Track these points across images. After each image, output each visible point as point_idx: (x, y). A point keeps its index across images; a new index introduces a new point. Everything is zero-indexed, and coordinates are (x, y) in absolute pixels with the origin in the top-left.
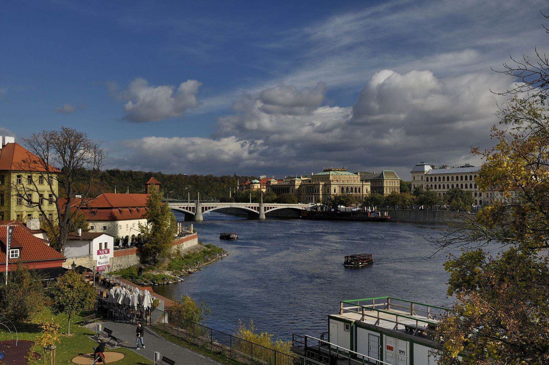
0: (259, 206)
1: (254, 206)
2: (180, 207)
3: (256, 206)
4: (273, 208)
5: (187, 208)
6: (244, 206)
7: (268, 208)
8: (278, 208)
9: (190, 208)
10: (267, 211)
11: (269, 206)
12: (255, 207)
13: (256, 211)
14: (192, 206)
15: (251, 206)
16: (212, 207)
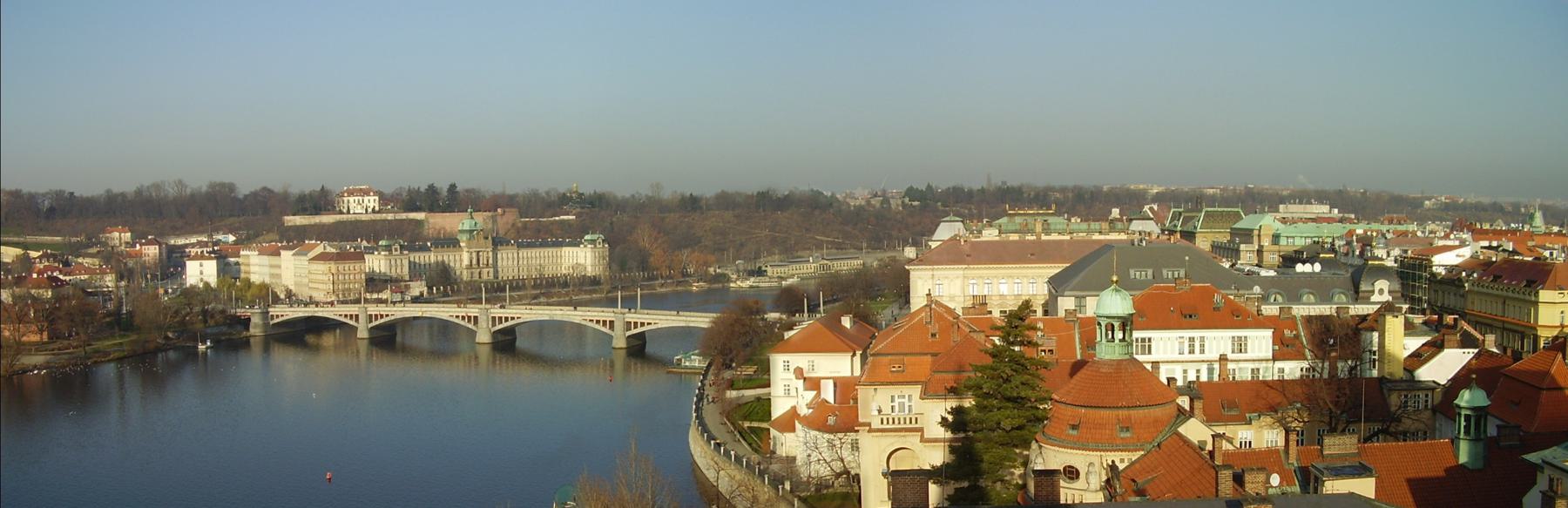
0: (613, 319)
1: (601, 319)
3: (608, 319)
4: (649, 324)
5: (463, 318)
6: (579, 318)
7: (636, 323)
8: (660, 326)
9: (469, 317)
10: (634, 331)
11: (639, 321)
12: (605, 322)
13: (606, 330)
14: (472, 315)
15: (595, 319)
16: (513, 318)
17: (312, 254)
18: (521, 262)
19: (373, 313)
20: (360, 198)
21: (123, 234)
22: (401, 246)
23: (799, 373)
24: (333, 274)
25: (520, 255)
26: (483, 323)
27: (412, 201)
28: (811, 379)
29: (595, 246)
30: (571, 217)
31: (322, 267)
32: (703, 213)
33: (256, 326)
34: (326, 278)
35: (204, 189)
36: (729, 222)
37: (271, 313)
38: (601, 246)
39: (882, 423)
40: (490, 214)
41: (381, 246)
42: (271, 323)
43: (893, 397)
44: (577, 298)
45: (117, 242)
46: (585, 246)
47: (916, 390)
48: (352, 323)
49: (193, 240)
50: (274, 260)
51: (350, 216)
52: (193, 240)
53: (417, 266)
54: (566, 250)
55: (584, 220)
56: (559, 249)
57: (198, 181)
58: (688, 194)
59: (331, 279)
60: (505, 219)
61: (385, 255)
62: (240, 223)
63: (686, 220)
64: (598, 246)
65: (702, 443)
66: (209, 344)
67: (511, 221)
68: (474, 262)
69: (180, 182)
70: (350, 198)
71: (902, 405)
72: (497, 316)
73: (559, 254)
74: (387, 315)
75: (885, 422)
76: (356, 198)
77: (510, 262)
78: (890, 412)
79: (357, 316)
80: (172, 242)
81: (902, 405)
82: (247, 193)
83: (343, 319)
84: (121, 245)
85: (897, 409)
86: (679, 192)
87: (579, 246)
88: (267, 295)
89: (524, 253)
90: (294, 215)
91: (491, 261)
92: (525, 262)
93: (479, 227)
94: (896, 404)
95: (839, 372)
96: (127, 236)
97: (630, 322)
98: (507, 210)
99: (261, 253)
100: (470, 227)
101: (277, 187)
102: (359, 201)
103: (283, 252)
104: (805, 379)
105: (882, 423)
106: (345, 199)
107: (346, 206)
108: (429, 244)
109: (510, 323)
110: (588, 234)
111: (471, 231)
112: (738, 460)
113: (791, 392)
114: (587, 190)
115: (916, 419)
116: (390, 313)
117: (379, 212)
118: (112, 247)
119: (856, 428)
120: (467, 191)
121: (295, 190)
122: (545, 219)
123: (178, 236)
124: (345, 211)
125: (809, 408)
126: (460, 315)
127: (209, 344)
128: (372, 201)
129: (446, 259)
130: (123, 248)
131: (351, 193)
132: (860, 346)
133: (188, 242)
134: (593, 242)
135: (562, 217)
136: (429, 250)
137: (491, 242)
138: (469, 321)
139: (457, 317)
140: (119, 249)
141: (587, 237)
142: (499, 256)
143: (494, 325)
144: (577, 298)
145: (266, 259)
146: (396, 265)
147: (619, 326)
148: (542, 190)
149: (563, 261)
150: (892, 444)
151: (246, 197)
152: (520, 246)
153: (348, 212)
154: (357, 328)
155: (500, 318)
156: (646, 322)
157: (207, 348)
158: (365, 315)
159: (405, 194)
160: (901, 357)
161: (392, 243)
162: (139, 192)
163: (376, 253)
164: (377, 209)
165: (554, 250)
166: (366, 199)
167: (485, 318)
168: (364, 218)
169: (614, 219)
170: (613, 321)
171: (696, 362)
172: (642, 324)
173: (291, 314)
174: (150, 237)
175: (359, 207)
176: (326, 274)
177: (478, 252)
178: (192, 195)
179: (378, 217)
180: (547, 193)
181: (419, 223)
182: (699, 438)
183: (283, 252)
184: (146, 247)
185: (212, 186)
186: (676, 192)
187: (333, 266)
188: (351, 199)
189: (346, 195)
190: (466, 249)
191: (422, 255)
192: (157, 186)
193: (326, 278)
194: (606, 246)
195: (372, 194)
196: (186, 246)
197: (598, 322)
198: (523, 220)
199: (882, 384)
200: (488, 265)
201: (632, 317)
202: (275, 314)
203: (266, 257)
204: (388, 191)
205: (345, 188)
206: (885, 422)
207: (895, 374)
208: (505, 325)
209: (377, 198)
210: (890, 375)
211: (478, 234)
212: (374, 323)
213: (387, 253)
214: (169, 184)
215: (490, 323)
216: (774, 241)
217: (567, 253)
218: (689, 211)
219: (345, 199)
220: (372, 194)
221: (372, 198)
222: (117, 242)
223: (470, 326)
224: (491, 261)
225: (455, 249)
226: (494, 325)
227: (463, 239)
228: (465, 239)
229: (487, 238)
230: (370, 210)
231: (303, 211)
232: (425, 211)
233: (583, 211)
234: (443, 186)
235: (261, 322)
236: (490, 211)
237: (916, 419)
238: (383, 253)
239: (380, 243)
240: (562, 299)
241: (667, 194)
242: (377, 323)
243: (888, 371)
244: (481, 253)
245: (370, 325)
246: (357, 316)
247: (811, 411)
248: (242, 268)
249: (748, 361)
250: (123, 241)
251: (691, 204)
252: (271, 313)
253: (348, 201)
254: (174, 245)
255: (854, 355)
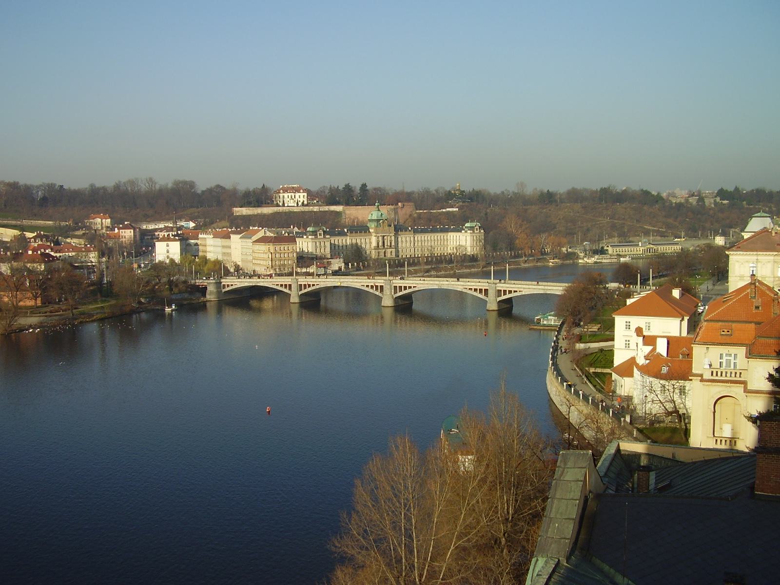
1: (478, 288)
2: (362, 285)
4: (515, 291)
5: (372, 287)
7: (505, 291)
8: (523, 293)
9: (377, 287)
10: (503, 297)
11: (507, 289)
12: (481, 290)
13: (482, 296)
14: (379, 285)
16: (410, 287)
17: (255, 238)
18: (416, 244)
19: (303, 283)
20: (293, 194)
21: (104, 220)
22: (324, 231)
23: (639, 331)
24: (271, 253)
25: (416, 239)
26: (387, 291)
27: (333, 197)
28: (649, 337)
29: (474, 232)
30: (455, 209)
31: (263, 247)
32: (557, 206)
33: (211, 293)
34: (266, 256)
35: (170, 185)
36: (578, 212)
37: (223, 283)
38: (478, 231)
39: (712, 375)
40: (392, 207)
41: (309, 231)
42: (223, 291)
43: (721, 355)
44: (459, 271)
45: (99, 227)
46: (466, 232)
47: (741, 351)
48: (286, 291)
49: (162, 226)
50: (225, 242)
51: (285, 208)
52: (162, 226)
53: (337, 248)
54: (452, 235)
55: (465, 211)
56: (445, 234)
57: (165, 179)
58: (546, 191)
59: (270, 257)
60: (404, 211)
61: (312, 239)
62: (199, 213)
63: (544, 210)
64: (476, 232)
65: (556, 384)
66: (174, 307)
67: (408, 213)
68: (381, 244)
69: (151, 179)
70: (284, 194)
71: (728, 363)
72: (398, 285)
73: (445, 238)
74: (313, 285)
75: (714, 374)
76: (290, 194)
77: (408, 244)
78: (719, 367)
79: (290, 286)
80: (144, 227)
81: (728, 363)
82: (204, 189)
83: (279, 288)
84: (102, 228)
85: (724, 364)
86: (538, 189)
87: (461, 232)
88: (220, 269)
89: (419, 237)
90: (241, 207)
91: (393, 244)
92: (420, 244)
93: (384, 217)
94: (724, 361)
95: (670, 332)
96: (108, 222)
97: (501, 290)
98: (406, 204)
99: (216, 236)
100: (377, 217)
101: (228, 185)
102: (291, 197)
103: (232, 236)
104: (644, 337)
105: (712, 375)
106: (281, 195)
107: (281, 200)
108: (346, 230)
109: (408, 291)
110: (468, 222)
111: (378, 221)
112: (586, 398)
113: (630, 345)
114: (468, 188)
115: (741, 373)
116: (316, 284)
117: (307, 205)
118: (95, 230)
119: (690, 378)
120: (375, 189)
121: (242, 187)
122: (435, 211)
123: (149, 222)
124: (281, 204)
125: (646, 359)
126: (370, 285)
127: (174, 307)
128: (302, 197)
129: (358, 241)
130: (104, 231)
131: (285, 190)
132: (688, 313)
133: (157, 227)
134: (472, 228)
135: (447, 209)
136: (345, 234)
137: (393, 229)
138: (377, 289)
139: (367, 286)
140: (101, 232)
141: (467, 225)
142: (400, 239)
143: (395, 292)
144: (459, 271)
145: (219, 242)
146: (320, 246)
147: (491, 293)
148: (432, 189)
149: (449, 243)
150: (719, 392)
151: (203, 192)
152: (416, 232)
153: (284, 205)
154: (290, 295)
155: (400, 287)
156: (513, 290)
157: (172, 311)
158: (296, 285)
159: (327, 191)
160: (730, 324)
161: (317, 229)
162: (117, 187)
163: (305, 237)
164: (306, 202)
165: (442, 235)
166: (297, 195)
167: (389, 287)
168: (296, 210)
169: (488, 211)
170: (487, 290)
171: (552, 320)
172: (510, 292)
173: (238, 284)
174: (126, 223)
175: (292, 201)
176: (266, 253)
177: (384, 236)
178: (161, 190)
179: (306, 209)
180: (437, 191)
181: (338, 214)
182: (554, 380)
183: (232, 236)
184: (123, 230)
185: (177, 183)
186: (536, 189)
187: (272, 247)
188: (286, 195)
189: (281, 191)
190: (374, 234)
191: (340, 238)
192: (132, 183)
193: (266, 256)
194: (482, 231)
195: (302, 191)
196: (156, 230)
197: (476, 290)
198: (417, 211)
199: (714, 344)
200: (391, 246)
201: (502, 286)
202: (226, 284)
203: (219, 240)
204: (314, 188)
205: (281, 187)
206: (714, 374)
207: (724, 337)
208: (404, 292)
209: (305, 194)
210: (720, 337)
211: (383, 222)
212: (304, 291)
213: (313, 237)
214: (142, 181)
215: (393, 291)
216: (613, 227)
217: (452, 237)
218: (547, 204)
219: (281, 195)
220: (302, 191)
221: (302, 195)
222: (99, 227)
223: (378, 293)
224: (393, 244)
225: (365, 234)
226: (395, 292)
227: (372, 227)
228: (373, 226)
229: (391, 226)
230: (300, 204)
231: (248, 204)
232: (342, 205)
233: (464, 204)
234: (356, 185)
235: (215, 291)
236: (392, 205)
237: (741, 373)
238: (310, 237)
239: (308, 229)
240: (448, 272)
241: (529, 191)
242: (306, 291)
243: (719, 334)
244: (385, 237)
245: (300, 293)
246: (290, 286)
247: (648, 361)
248: (200, 248)
249: (593, 321)
250: (104, 226)
251: (548, 198)
252: (223, 283)
253: (284, 196)
254: (146, 230)
255: (683, 319)
